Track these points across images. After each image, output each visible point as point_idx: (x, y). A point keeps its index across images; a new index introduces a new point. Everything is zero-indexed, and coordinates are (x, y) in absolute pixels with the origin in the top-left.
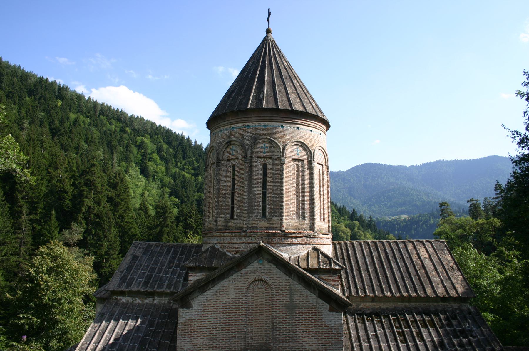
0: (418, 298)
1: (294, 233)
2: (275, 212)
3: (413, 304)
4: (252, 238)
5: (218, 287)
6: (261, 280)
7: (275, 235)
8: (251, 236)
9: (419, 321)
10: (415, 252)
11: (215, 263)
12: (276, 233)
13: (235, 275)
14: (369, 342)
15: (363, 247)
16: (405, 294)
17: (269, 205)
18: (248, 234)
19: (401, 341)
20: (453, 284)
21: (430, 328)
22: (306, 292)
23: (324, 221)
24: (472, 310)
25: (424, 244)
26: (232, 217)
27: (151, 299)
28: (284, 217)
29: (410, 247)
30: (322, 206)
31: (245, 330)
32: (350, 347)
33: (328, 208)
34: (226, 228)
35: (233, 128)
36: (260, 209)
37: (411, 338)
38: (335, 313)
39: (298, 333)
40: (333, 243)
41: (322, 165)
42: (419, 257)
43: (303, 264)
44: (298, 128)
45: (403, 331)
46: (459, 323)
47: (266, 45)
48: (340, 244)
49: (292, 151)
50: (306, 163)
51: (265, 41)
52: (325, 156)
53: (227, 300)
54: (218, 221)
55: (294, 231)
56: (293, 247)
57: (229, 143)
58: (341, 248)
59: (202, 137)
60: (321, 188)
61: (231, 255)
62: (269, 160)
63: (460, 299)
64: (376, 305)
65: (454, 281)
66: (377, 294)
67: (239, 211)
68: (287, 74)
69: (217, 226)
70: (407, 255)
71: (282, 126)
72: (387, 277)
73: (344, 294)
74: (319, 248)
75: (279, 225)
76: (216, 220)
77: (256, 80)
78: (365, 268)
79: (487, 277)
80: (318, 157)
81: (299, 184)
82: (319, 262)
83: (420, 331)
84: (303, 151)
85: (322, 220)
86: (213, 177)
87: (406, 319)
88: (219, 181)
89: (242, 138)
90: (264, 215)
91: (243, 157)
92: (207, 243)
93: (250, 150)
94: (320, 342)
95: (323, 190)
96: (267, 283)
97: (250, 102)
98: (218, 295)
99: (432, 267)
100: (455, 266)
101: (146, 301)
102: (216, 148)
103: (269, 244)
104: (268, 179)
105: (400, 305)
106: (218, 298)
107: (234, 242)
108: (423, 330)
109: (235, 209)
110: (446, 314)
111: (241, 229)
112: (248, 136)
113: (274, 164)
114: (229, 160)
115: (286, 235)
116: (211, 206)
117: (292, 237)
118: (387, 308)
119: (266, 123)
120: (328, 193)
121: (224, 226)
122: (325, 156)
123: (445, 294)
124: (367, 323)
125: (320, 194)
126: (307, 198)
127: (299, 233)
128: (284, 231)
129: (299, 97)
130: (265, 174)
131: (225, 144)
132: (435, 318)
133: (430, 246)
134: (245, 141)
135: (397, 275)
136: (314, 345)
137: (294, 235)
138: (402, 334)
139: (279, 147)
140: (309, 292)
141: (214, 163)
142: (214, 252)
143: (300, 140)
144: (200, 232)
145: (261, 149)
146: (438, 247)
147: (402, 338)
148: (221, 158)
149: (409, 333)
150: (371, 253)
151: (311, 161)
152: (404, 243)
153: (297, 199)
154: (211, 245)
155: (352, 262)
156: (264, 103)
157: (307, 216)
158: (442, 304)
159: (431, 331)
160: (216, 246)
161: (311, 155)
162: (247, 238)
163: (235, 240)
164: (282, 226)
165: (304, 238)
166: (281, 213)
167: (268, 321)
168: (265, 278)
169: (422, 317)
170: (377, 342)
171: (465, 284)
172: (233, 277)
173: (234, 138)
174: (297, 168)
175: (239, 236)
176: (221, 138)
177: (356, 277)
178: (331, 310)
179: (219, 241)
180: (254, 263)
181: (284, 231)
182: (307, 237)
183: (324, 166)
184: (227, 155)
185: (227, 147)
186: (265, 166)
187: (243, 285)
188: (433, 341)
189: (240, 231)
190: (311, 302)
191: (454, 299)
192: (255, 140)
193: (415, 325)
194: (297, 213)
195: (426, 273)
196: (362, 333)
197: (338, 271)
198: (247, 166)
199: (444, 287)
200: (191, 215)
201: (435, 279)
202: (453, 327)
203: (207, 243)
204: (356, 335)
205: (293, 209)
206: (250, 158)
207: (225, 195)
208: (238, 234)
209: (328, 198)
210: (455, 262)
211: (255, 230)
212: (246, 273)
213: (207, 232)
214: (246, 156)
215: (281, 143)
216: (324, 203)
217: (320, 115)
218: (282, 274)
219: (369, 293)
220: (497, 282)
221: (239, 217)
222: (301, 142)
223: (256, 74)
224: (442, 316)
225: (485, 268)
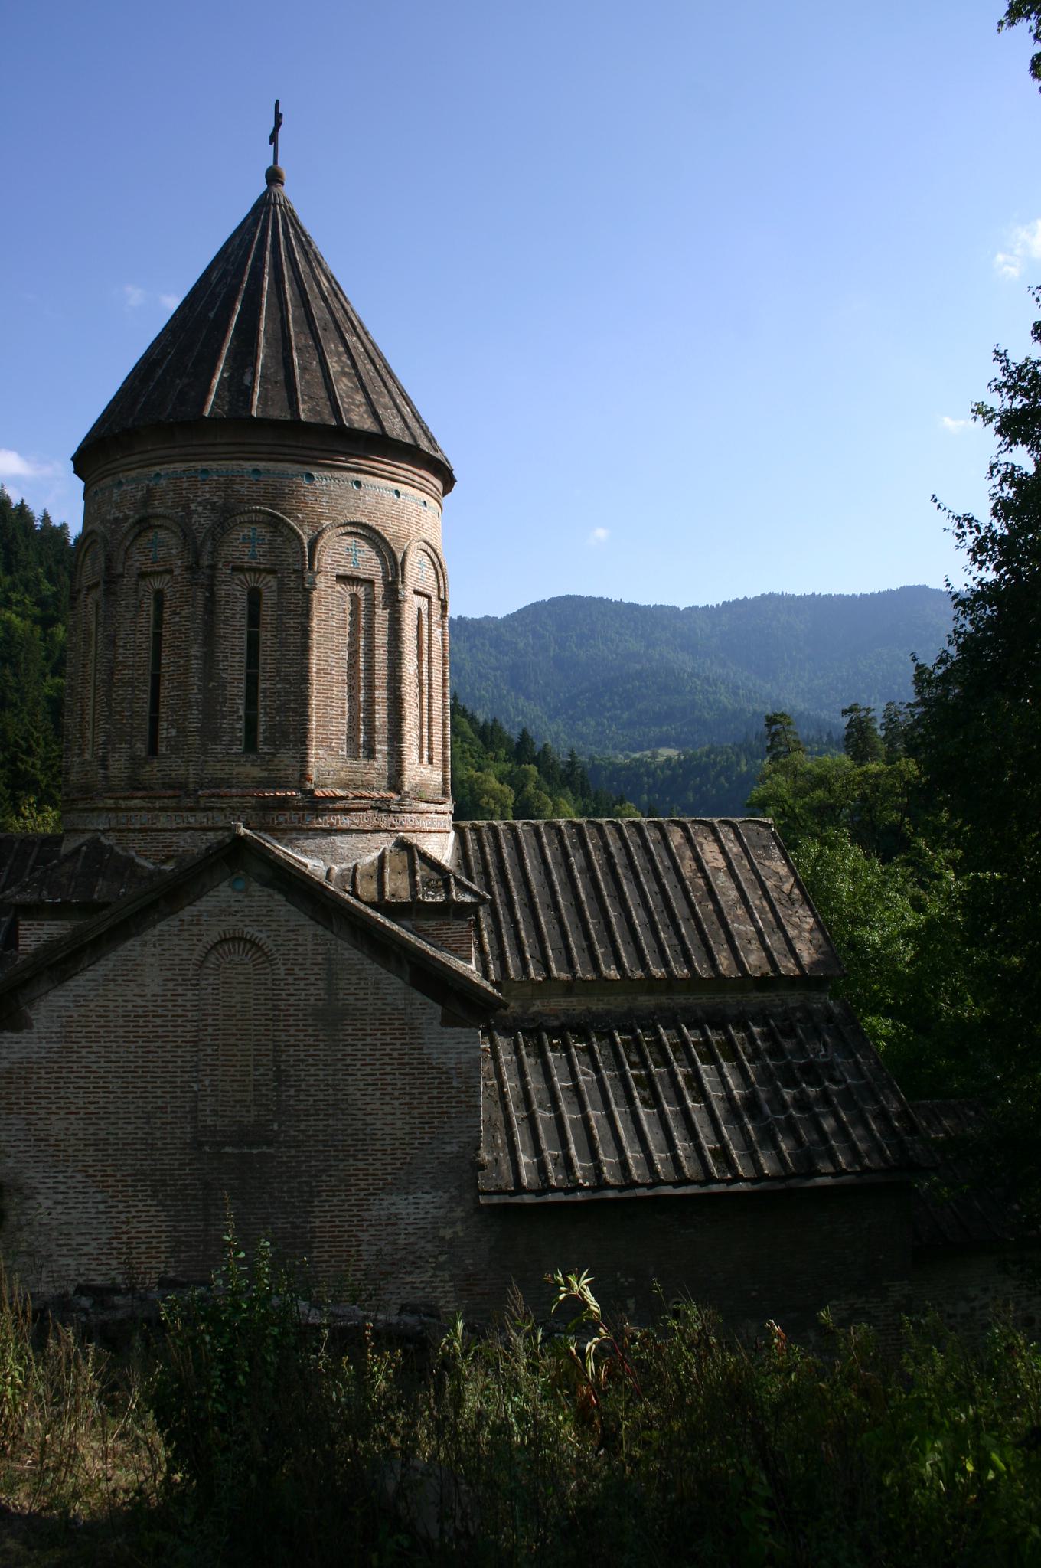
0: (694, 983)
3: (681, 1000)
4: (216, 813)
5: (111, 964)
6: (240, 939)
7: (283, 804)
8: (211, 809)
9: (695, 1043)
10: (689, 854)
11: (101, 890)
12: (286, 798)
13: (162, 926)
14: (556, 1108)
15: (544, 840)
16: (658, 972)
17: (266, 714)
18: (203, 803)
19: (644, 1102)
20: (789, 942)
21: (725, 1064)
22: (374, 970)
23: (430, 762)
24: (836, 1010)
25: (714, 831)
26: (153, 750)
29: (676, 838)
31: (195, 1087)
32: (501, 1125)
34: (135, 785)
35: (158, 475)
36: (240, 725)
37: (671, 1093)
38: (458, 1029)
39: (351, 1089)
40: (456, 827)
41: (429, 597)
42: (701, 868)
43: (368, 889)
44: (358, 484)
45: (650, 1075)
46: (801, 1048)
47: (266, 220)
48: (476, 830)
49: (338, 554)
50: (379, 591)
51: (265, 206)
52: (439, 569)
53: (139, 1001)
55: (340, 793)
56: (338, 839)
57: (144, 524)
58: (479, 841)
59: (61, 502)
60: (425, 665)
61: (151, 866)
62: (269, 578)
63: (805, 981)
64: (576, 1005)
65: (792, 932)
66: (580, 974)
67: (173, 732)
68: (328, 317)
69: (106, 778)
70: (667, 863)
71: (310, 477)
72: (608, 925)
73: (486, 975)
74: (414, 842)
75: (297, 775)
77: (232, 328)
78: (548, 900)
79: (881, 920)
80: (417, 573)
81: (357, 652)
82: (413, 884)
83: (696, 1071)
84: (372, 554)
85: (425, 760)
86: (93, 627)
87: (658, 1042)
88: (112, 642)
89: (186, 507)
90: (251, 745)
91: (188, 568)
92: (76, 831)
94: (415, 1112)
96: (259, 948)
97: (212, 397)
98: (112, 985)
99: (734, 894)
100: (796, 891)
103: (266, 830)
104: (265, 635)
105: (646, 1002)
106: (110, 996)
107: (159, 825)
108: (703, 1068)
109: (164, 725)
110: (768, 1024)
112: (204, 504)
113: (281, 589)
114: (142, 576)
115: (317, 805)
116: (89, 718)
118: (608, 1012)
119: (261, 465)
120: (444, 681)
121: (129, 777)
122: (439, 569)
123: (767, 968)
124: (550, 1054)
125: (420, 685)
126: (381, 695)
127: (356, 797)
129: (363, 387)
130: (254, 619)
132: (738, 1036)
133: (732, 837)
135: (638, 917)
136: (399, 1124)
137: (340, 804)
138: (647, 1082)
139: (299, 537)
140: (383, 971)
141: (97, 585)
142: (98, 859)
143: (365, 520)
144: (59, 797)
145: (244, 544)
146: (754, 839)
147: (646, 1093)
148: (120, 570)
149: (667, 1079)
150: (566, 855)
151: (395, 583)
152: (659, 826)
153: (352, 698)
154: (88, 836)
155: (512, 883)
156: (255, 403)
157: (382, 747)
158: (757, 997)
159: (726, 1071)
160: (102, 839)
162: (200, 815)
163: (163, 821)
164: (304, 776)
165: (370, 813)
166: (301, 739)
167: (264, 1060)
168: (251, 931)
169: (704, 1033)
170: (577, 1108)
171: (821, 941)
172: (156, 932)
174: (352, 602)
175: (175, 810)
177: (521, 926)
178: (448, 1021)
179: (113, 823)
180: (221, 888)
181: (312, 792)
182: (381, 810)
183: (434, 600)
184: (139, 560)
185: (139, 535)
186: (255, 597)
187: (185, 955)
188: (729, 1098)
189: (177, 793)
190: (390, 999)
191: (790, 982)
192: (227, 514)
193: (684, 1056)
195: (719, 911)
196: (534, 1083)
197: (472, 908)
198: (201, 594)
199: (766, 949)
200: (30, 747)
201: (742, 928)
202: (784, 1057)
203: (76, 831)
204: (519, 1089)
205: (339, 726)
206: (208, 571)
208: (172, 803)
209: (444, 695)
210: (797, 880)
211: (224, 791)
212: (196, 921)
214: (197, 563)
215: (306, 529)
216: (430, 710)
217: (424, 445)
218: (304, 920)
219: (559, 970)
220: (908, 934)
222: (364, 526)
223: (233, 310)
224: (756, 1030)
225: (879, 896)
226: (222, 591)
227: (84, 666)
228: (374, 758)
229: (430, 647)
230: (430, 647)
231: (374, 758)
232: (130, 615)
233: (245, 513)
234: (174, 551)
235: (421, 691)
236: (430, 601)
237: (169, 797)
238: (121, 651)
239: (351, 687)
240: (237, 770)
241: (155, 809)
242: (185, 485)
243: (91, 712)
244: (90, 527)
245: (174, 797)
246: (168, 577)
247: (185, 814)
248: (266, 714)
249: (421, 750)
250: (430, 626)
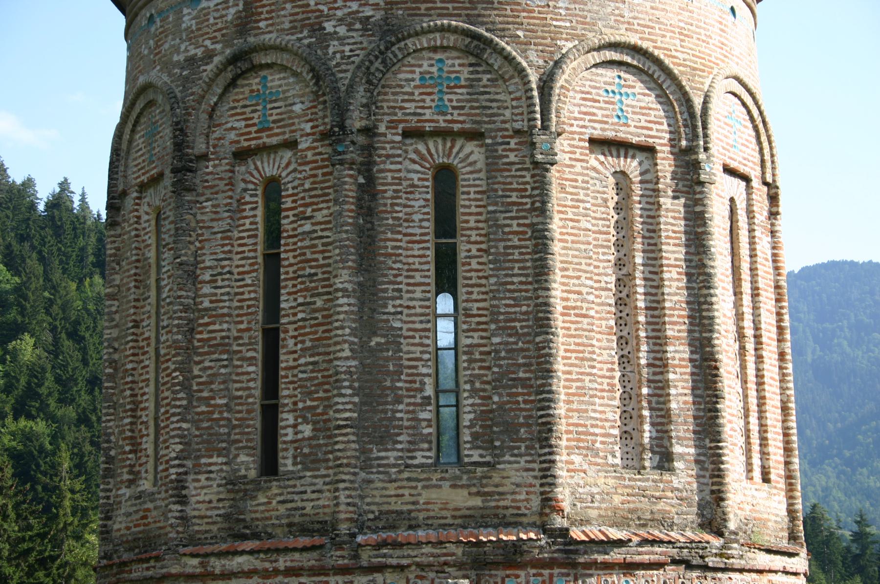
1: (620, 543)
2: (511, 429)
8: (380, 568)
12: (517, 547)
17: (474, 392)
18: (366, 557)
23: (766, 479)
26: (269, 465)
28: (561, 458)
30: (753, 401)
33: (785, 409)
34: (238, 530)
41: (746, 179)
50: (666, 165)
52: (760, 127)
54: (192, 489)
55: (615, 534)
57: (242, 64)
60: (747, 299)
67: (307, 430)
69: (184, 519)
76: (180, 484)
80: (728, 138)
81: (631, 276)
84: (650, 100)
85: (757, 474)
86: (152, 254)
88: (190, 274)
89: (317, 29)
91: (325, 136)
93: (360, 95)
95: (756, 315)
102: (170, 95)
109: (287, 418)
111: (322, 532)
112: (348, 21)
113: (493, 166)
114: (241, 155)
116: (148, 416)
117: (608, 567)
120: (780, 329)
121: (227, 517)
122: (760, 127)
125: (741, 336)
126: (678, 352)
127: (645, 542)
128: (564, 532)
130: (445, 221)
131: (220, 71)
134: (334, 46)
137: (616, 555)
139: (521, 72)
141: (156, 180)
143: (633, 39)
148: (200, 147)
151: (691, 150)
153: (626, 360)
157: (684, 449)
161: (690, 122)
164: (549, 503)
165: (671, 571)
166: (543, 435)
174: (619, 187)
176: (192, 37)
181: (564, 532)
182: (689, 566)
183: (756, 183)
184: (233, 130)
185: (233, 84)
186: (445, 179)
189: (317, 540)
194: (626, 435)
198: (350, 181)
205: (607, 412)
206: (361, 139)
207: (223, 346)
208: (308, 560)
209: (782, 355)
211: (402, 535)
213: (126, 557)
214: (342, 127)
215: (532, 55)
216: (760, 384)
221: (310, 462)
222: (635, 50)
226: (387, 172)
227: (137, 324)
228: (671, 470)
229: (753, 270)
230: (753, 270)
231: (671, 470)
232: (223, 225)
233: (424, 32)
234: (297, 108)
235: (742, 348)
236: (749, 187)
237: (305, 549)
238: (206, 289)
239: (622, 341)
241: (276, 572)
243: (151, 405)
244: (141, 80)
245: (313, 548)
246: (288, 154)
248: (474, 392)
249: (749, 458)
250: (751, 231)
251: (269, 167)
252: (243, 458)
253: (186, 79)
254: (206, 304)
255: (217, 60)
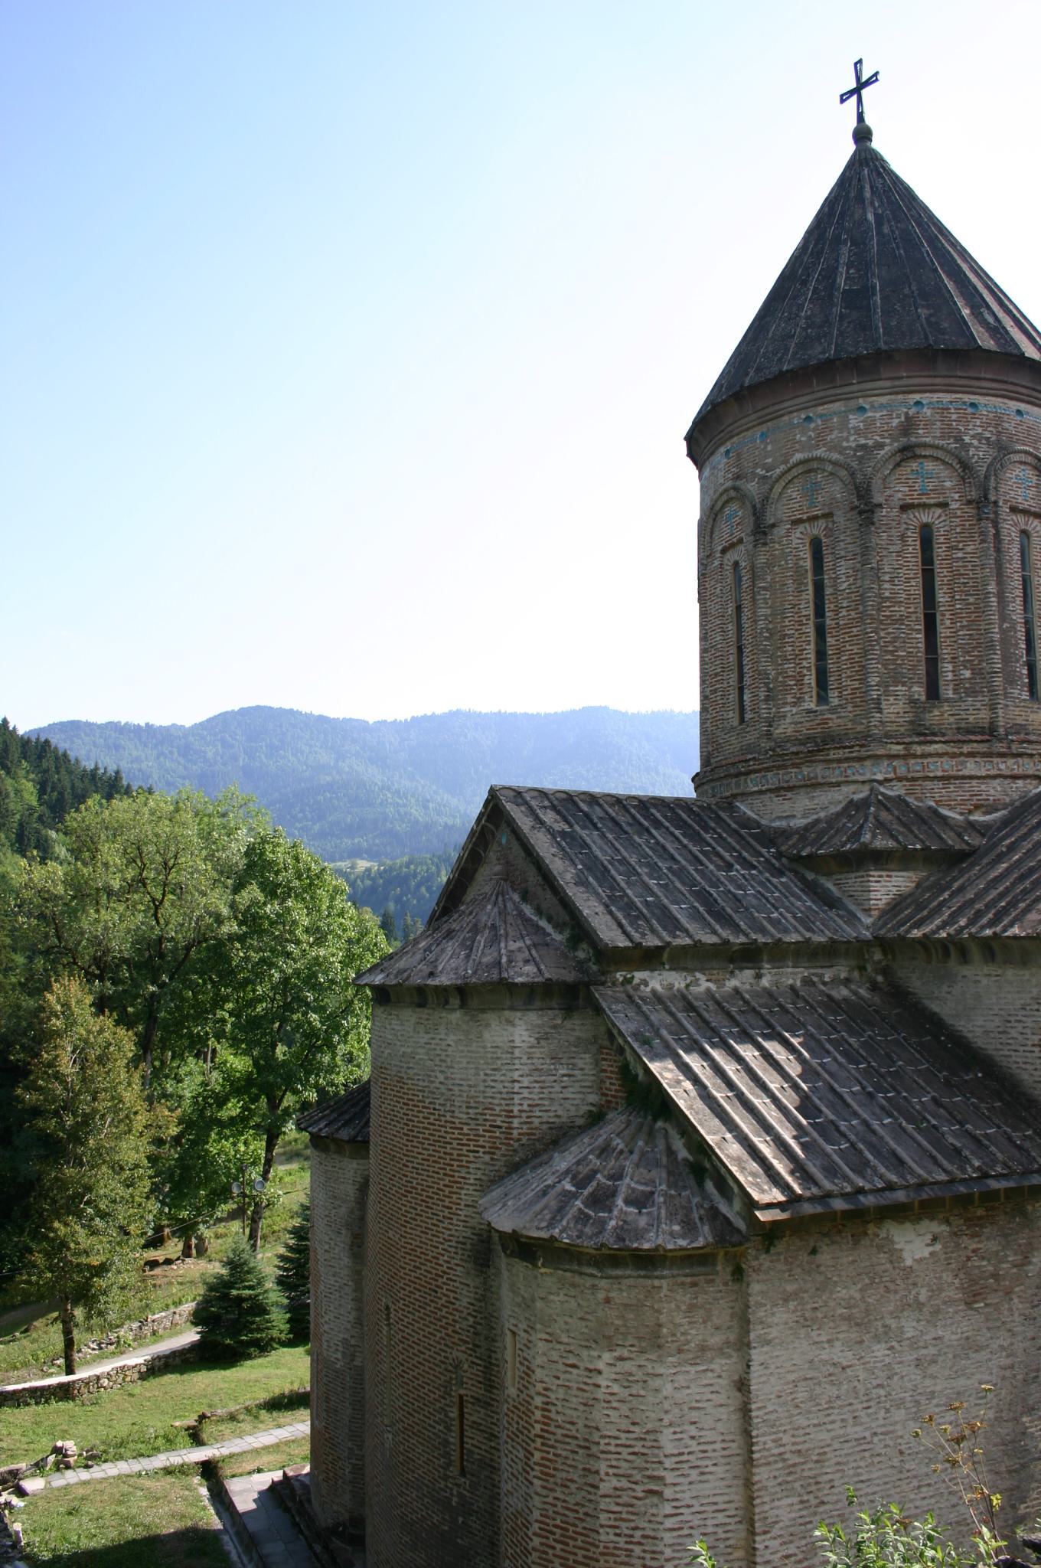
4: (1026, 760)
8: (1020, 755)
18: (1015, 748)
26: (933, 691)
27: (748, 974)
35: (918, 403)
67: (967, 674)
89: (959, 439)
101: (732, 983)
107: (966, 772)
112: (978, 437)
114: (905, 508)
121: (911, 722)
162: (1011, 761)
173: (923, 436)
175: (984, 755)
179: (902, 771)
184: (900, 491)
185: (898, 465)
207: (900, 621)
214: (986, 498)
232: (897, 548)
237: (982, 741)
240: (1032, 717)
241: (962, 754)
242: (954, 417)
246: (939, 511)
247: (995, 760)
251: (925, 518)
252: (916, 688)
253: (862, 457)
254: (887, 594)
255: (887, 448)
